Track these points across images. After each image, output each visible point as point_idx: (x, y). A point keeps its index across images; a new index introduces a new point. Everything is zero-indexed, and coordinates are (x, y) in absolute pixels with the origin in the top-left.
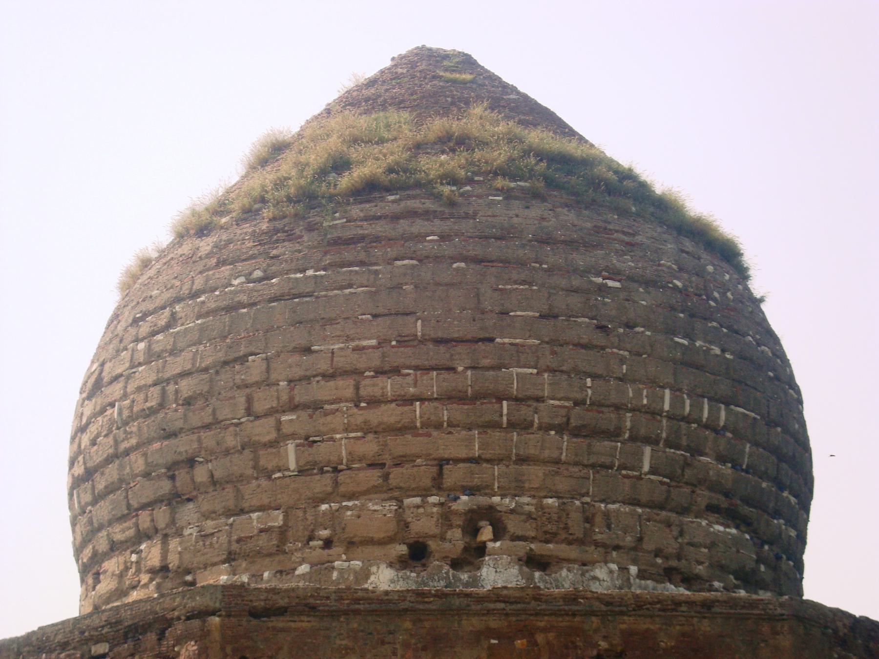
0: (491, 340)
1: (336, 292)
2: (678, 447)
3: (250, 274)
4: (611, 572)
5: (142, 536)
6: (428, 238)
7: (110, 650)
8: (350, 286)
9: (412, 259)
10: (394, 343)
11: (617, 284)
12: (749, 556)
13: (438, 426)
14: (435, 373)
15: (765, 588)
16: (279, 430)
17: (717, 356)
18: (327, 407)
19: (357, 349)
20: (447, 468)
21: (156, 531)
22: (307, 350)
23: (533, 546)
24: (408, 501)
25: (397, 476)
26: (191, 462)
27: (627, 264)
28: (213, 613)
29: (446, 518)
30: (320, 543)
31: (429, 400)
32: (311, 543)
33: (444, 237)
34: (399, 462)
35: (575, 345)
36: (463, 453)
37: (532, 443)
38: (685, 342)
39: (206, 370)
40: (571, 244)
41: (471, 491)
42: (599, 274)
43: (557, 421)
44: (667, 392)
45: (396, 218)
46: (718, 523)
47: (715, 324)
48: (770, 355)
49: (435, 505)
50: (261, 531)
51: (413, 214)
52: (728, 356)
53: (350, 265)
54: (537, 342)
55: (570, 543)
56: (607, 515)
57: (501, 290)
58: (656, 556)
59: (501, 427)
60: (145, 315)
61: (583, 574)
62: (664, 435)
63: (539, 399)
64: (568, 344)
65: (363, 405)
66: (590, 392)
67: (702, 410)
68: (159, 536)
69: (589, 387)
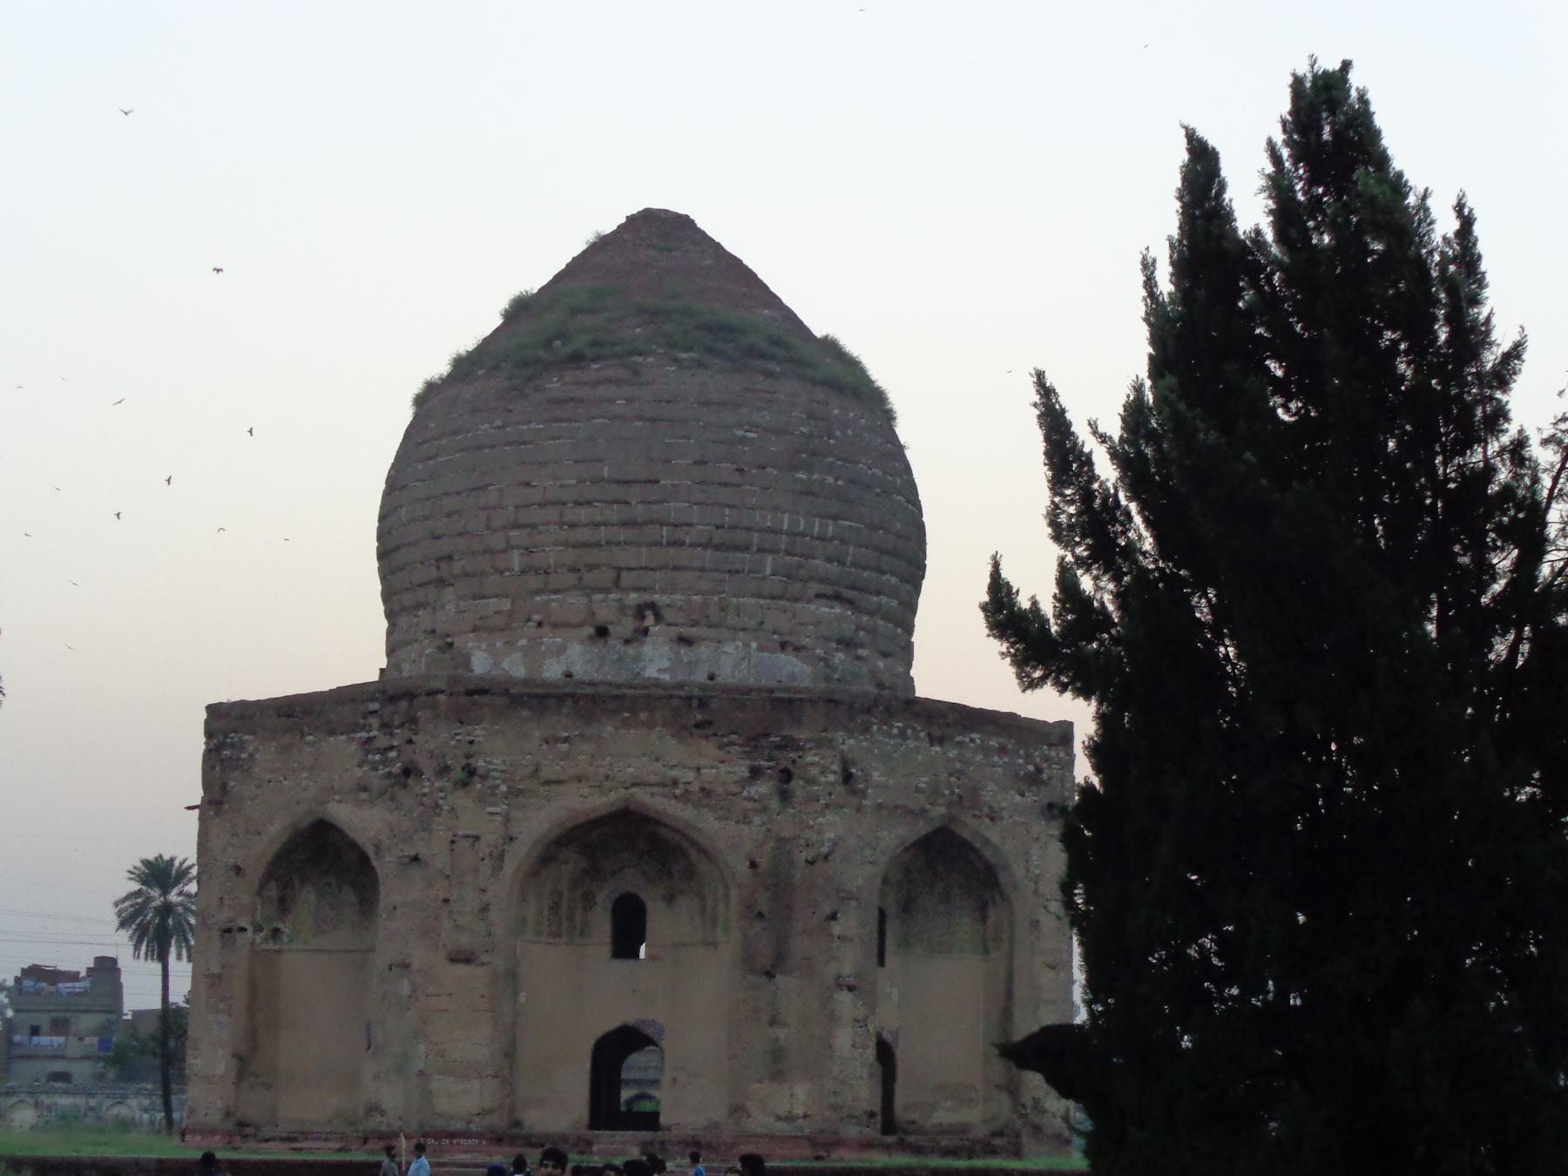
0: (657, 482)
1: (551, 442)
2: (794, 555)
3: (493, 422)
4: (737, 648)
5: (420, 605)
6: (618, 402)
7: (381, 709)
8: (560, 438)
9: (604, 418)
10: (588, 483)
11: (755, 435)
12: (848, 629)
13: (618, 544)
14: (615, 506)
15: (861, 645)
16: (508, 542)
17: (830, 484)
18: (540, 527)
19: (562, 486)
20: (624, 574)
21: (429, 604)
22: (527, 484)
23: (681, 630)
24: (597, 597)
25: (591, 578)
26: (450, 558)
27: (765, 418)
28: (442, 692)
29: (622, 609)
30: (535, 624)
31: (613, 525)
32: (530, 623)
33: (630, 400)
34: (590, 568)
35: (719, 484)
36: (634, 565)
37: (683, 556)
38: (805, 477)
39: (459, 493)
40: (723, 404)
41: (638, 589)
42: (741, 427)
43: (703, 540)
44: (786, 516)
45: (596, 384)
46: (826, 606)
47: (831, 459)
48: (880, 473)
49: (613, 600)
50: (496, 612)
51: (608, 380)
52: (840, 483)
53: (561, 420)
54: (689, 483)
55: (710, 627)
56: (738, 607)
57: (667, 443)
58: (774, 633)
59: (662, 545)
60: (424, 442)
61: (716, 650)
62: (783, 547)
63: (690, 525)
64: (713, 483)
65: (565, 527)
66: (727, 519)
67: (813, 527)
68: (429, 609)
69: (728, 516)
